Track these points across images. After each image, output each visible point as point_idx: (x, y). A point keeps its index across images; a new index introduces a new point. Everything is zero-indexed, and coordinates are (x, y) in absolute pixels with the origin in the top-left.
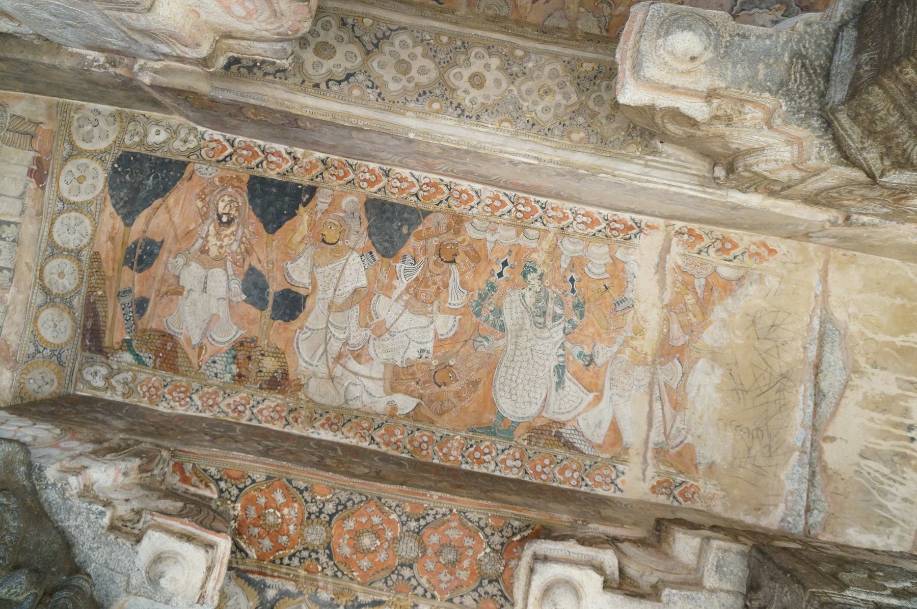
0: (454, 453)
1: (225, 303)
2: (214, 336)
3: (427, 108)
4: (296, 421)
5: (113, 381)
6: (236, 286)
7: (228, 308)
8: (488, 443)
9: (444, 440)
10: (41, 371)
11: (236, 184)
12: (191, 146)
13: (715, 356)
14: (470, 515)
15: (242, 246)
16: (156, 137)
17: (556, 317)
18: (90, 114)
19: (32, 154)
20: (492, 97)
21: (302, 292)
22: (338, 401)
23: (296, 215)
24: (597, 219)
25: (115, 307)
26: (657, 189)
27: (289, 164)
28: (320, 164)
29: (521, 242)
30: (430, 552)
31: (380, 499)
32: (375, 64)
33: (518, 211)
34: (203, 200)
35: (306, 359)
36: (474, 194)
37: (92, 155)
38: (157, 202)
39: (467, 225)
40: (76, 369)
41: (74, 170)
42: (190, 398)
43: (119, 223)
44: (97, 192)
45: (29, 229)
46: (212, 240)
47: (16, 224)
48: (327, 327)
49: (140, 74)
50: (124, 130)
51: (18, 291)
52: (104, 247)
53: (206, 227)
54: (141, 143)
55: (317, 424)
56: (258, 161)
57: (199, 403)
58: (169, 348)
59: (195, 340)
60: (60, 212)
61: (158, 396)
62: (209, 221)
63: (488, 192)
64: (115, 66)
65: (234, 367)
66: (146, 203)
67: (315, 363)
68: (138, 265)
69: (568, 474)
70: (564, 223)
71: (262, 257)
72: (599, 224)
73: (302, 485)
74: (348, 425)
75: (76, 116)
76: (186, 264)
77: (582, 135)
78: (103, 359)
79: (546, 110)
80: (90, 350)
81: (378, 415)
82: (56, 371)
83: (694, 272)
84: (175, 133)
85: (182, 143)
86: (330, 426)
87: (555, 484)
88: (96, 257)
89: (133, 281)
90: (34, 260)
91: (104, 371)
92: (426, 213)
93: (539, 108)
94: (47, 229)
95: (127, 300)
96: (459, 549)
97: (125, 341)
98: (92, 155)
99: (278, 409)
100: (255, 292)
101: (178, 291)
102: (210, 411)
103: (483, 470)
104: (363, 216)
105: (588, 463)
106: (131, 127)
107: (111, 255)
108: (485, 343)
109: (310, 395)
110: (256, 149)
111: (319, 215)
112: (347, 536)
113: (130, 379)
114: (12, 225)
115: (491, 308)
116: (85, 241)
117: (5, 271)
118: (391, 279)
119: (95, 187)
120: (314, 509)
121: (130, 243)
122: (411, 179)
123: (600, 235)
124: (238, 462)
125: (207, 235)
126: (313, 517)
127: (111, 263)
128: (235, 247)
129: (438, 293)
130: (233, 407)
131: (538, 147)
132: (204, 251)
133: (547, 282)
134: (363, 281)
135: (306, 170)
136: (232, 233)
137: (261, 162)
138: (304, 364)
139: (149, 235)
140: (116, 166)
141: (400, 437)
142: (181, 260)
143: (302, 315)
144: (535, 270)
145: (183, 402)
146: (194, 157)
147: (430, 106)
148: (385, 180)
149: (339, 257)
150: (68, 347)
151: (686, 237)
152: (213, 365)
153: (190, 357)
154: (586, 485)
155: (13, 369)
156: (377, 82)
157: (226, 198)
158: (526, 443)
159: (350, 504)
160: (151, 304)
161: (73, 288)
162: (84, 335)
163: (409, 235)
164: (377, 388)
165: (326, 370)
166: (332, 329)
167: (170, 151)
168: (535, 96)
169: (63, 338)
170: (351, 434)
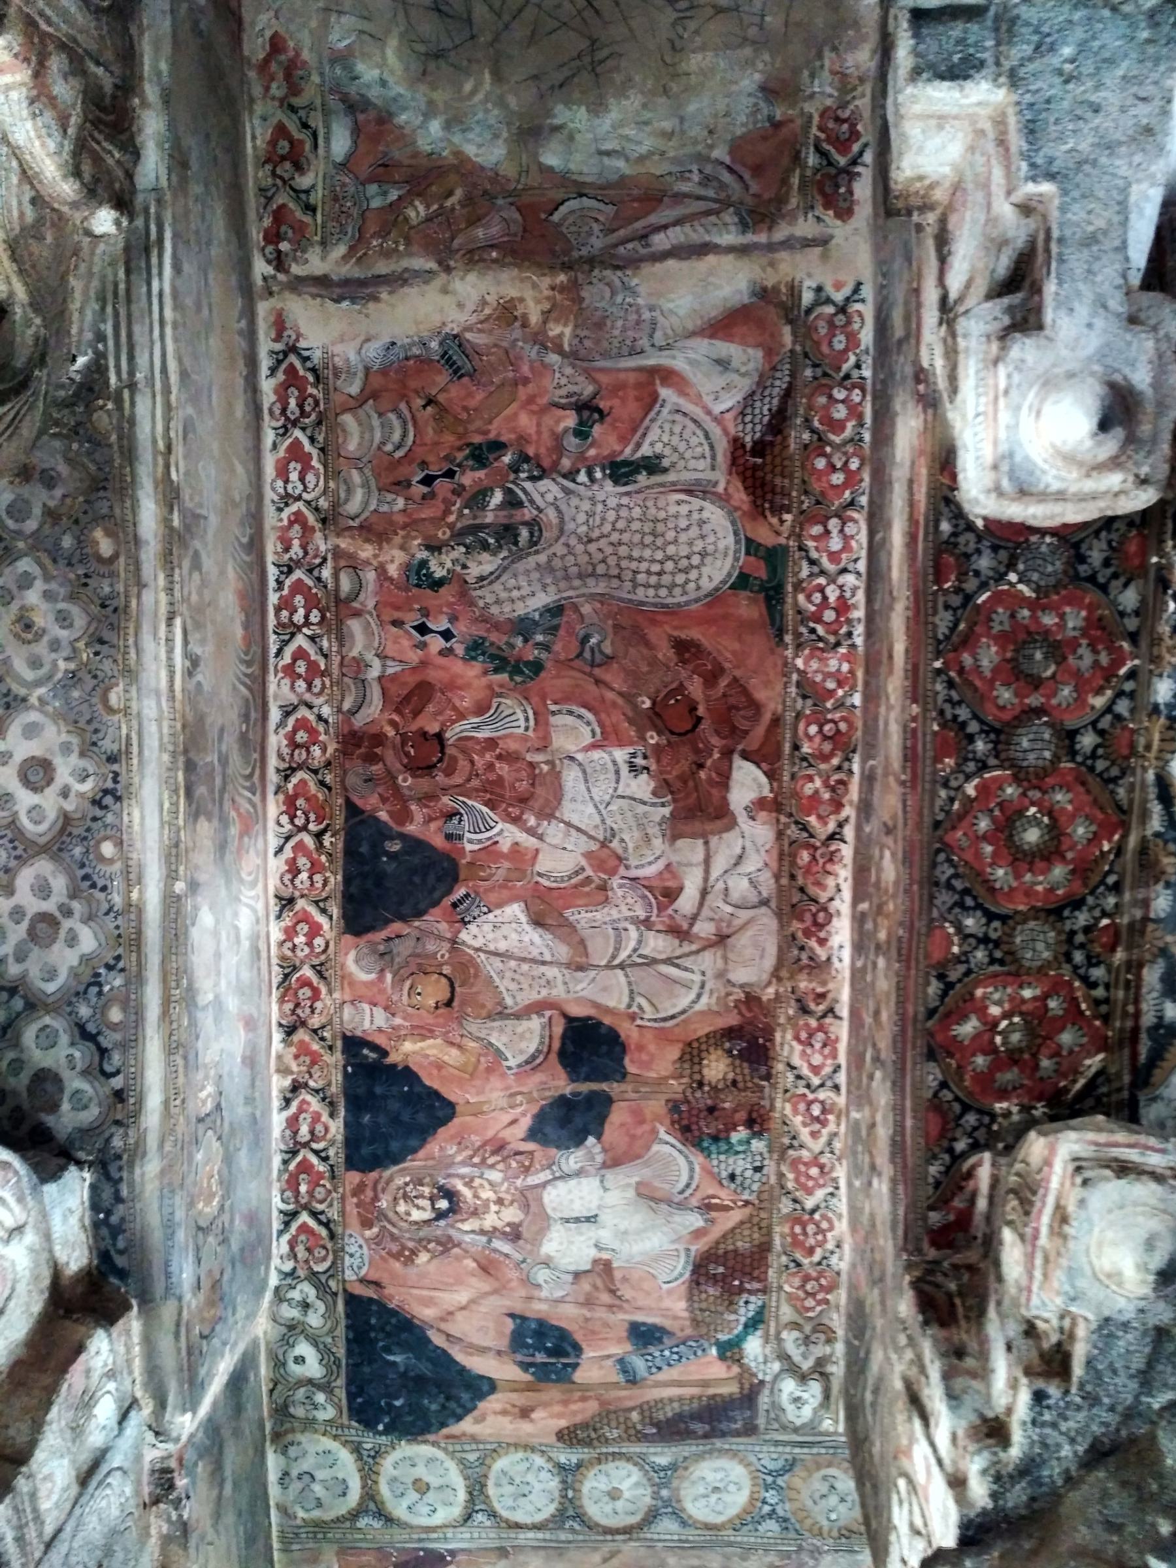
0: (833, 665)
2: (681, 1186)
3: (118, 866)
4: (822, 996)
6: (573, 1159)
7: (618, 1170)
8: (801, 598)
9: (808, 690)
10: (809, 1503)
11: (369, 1193)
13: (530, 132)
14: (942, 630)
15: (490, 1161)
17: (512, 502)
20: (64, 737)
21: (559, 1029)
22: (767, 921)
24: (289, 449)
25: (658, 1385)
26: (177, 351)
27: (309, 1098)
28: (296, 1038)
29: (371, 604)
30: (1034, 700)
31: (937, 825)
32: (51, 988)
33: (307, 623)
34: (414, 1253)
35: (692, 996)
36: (291, 721)
37: (369, 1473)
38: (438, 1340)
39: (359, 721)
41: (405, 1503)
42: (813, 1211)
43: (492, 1403)
44: (440, 1454)
46: (490, 1221)
48: (621, 966)
50: (309, 1424)
52: (547, 1421)
53: (467, 1238)
55: (822, 953)
56: (314, 1160)
57: (820, 1194)
58: (721, 1270)
59: (696, 1221)
60: (493, 1514)
63: (279, 690)
65: (735, 1137)
66: (443, 1359)
67: (697, 978)
68: (567, 1355)
69: (840, 412)
70: (311, 519)
71: (506, 1118)
72: (297, 443)
73: (934, 988)
74: (812, 890)
75: (301, 1514)
76: (547, 1263)
77: (98, 534)
78: (766, 1392)
79: (63, 619)
81: (780, 835)
82: (803, 1474)
83: (355, 212)
85: (310, 1312)
86: (821, 926)
87: (867, 436)
88: (567, 1436)
90: (596, 1549)
92: (352, 809)
93: (63, 634)
94: (531, 1535)
96: (1020, 639)
97: (722, 1357)
98: (369, 1473)
99: (804, 1035)
100: (578, 1121)
101: (603, 1268)
102: (832, 1169)
103: (860, 597)
104: (383, 934)
105: (808, 373)
106: (299, 1412)
107: (557, 1408)
108: (593, 641)
109: (765, 977)
110: (292, 1167)
111: (398, 1021)
112: (1028, 877)
113: (796, 1334)
115: (519, 642)
116: (539, 1461)
118: (501, 855)
119: (431, 1460)
120: (980, 955)
121: (528, 1377)
122: (288, 852)
123: (321, 438)
124: (909, 1123)
125: (482, 1232)
126: (998, 954)
127: (574, 1407)
128: (495, 1176)
129: (509, 757)
130: (817, 1126)
131: (146, 627)
132: (514, 1234)
133: (443, 534)
134: (515, 910)
135: (314, 1063)
136: (469, 1184)
137: (316, 1153)
138: (704, 1000)
139: (504, 1343)
140: (381, 1427)
141: (818, 783)
142: (542, 1275)
143: (607, 1021)
144: (424, 564)
145: (824, 1225)
146: (332, 1284)
147: (111, 861)
148: (301, 904)
149: (477, 967)
150: (753, 1459)
151: (284, 246)
152: (739, 1180)
153: (730, 1224)
154: (858, 366)
156: (87, 978)
157: (402, 1207)
158: (788, 517)
159: (958, 884)
160: (640, 1318)
161: (635, 1469)
162: (723, 1434)
163: (403, 837)
164: (726, 847)
165: (708, 956)
166: (623, 955)
167: (331, 1331)
168: (41, 648)
169: (737, 1471)
170: (830, 882)
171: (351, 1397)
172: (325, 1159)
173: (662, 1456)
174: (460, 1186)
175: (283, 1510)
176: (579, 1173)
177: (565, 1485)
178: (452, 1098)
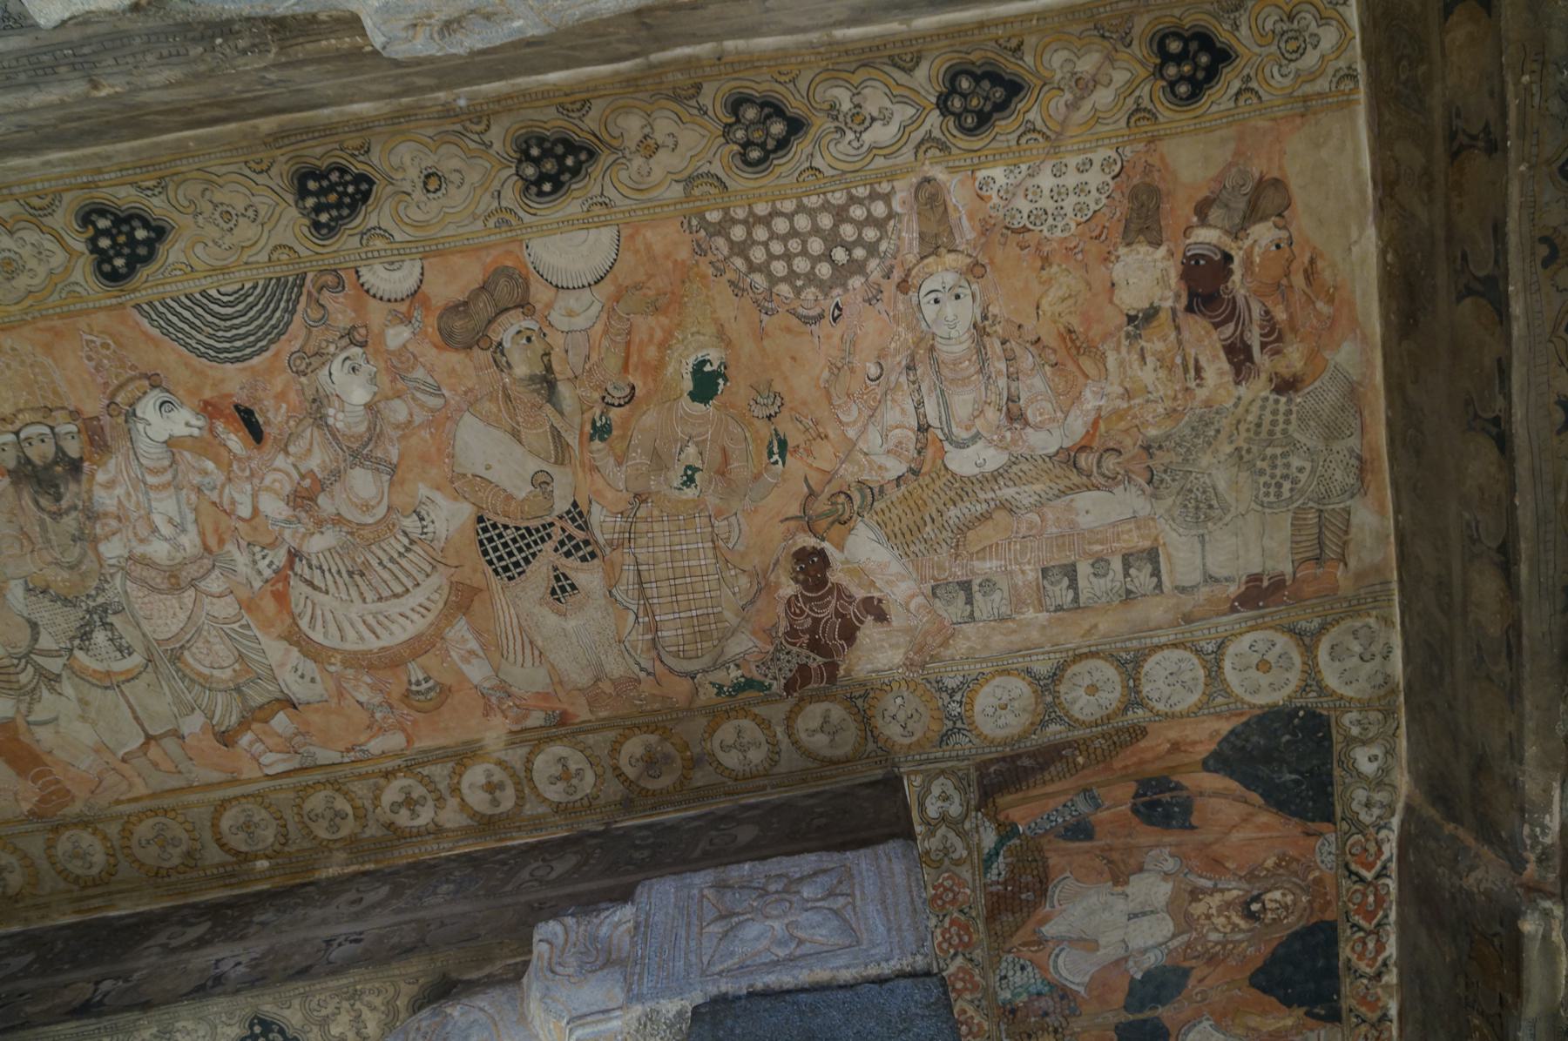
1: (1121, 953)
2: (1063, 954)
5: (943, 830)
6: (1152, 960)
10: (921, 709)
11: (1316, 905)
12: (1365, 817)
15: (1218, 948)
16: (1365, 761)
18: (1382, 641)
19: (1288, 568)
23: (1289, 1006)
25: (1065, 792)
27: (1368, 970)
28: (1379, 1013)
34: (1278, 865)
37: (1311, 671)
38: (1256, 798)
40: (942, 765)
41: (1277, 650)
42: (956, 954)
43: (1203, 751)
44: (1248, 698)
45: (1156, 611)
46: (1216, 900)
47: (1159, 585)
49: (1536, 915)
50: (1365, 706)
51: (1044, 627)
53: (1234, 884)
54: (1350, 741)
56: (1362, 923)
58: (1023, 896)
59: (1048, 930)
60: (1199, 652)
61: (943, 907)
62: (1246, 886)
64: (1539, 861)
65: (1024, 997)
68: (1144, 804)
71: (1208, 982)
75: (1372, 621)
76: (1167, 876)
80: (981, 776)
84: (1378, 784)
85: (1364, 800)
88: (1138, 732)
89: (1115, 806)
90: (1104, 636)
91: (955, 809)
94: (1164, 640)
95: (1083, 807)
97: (1014, 826)
98: (1311, 671)
101: (1119, 878)
106: (1374, 716)
107: (1149, 755)
113: (956, 856)
114: (1155, 580)
116: (1160, 707)
117: (1071, 594)
119: (1255, 692)
121: (1175, 778)
125: (1222, 891)
127: (1135, 759)
128: (1214, 936)
132: (1195, 894)
135: (1364, 997)
136: (1235, 926)
137: (1361, 929)
139: (1198, 802)
140: (1301, 713)
142: (1171, 865)
145: (945, 946)
146: (1345, 826)
153: (1020, 933)
155: (909, 664)
160: (1086, 845)
161: (1077, 715)
162: (1004, 759)
169: (988, 727)
171: (1328, 737)
172: (1353, 925)
173: (1055, 731)
174: (1243, 924)
175: (1387, 621)
176: (1145, 951)
177: (1136, 690)
178: (1253, 990)
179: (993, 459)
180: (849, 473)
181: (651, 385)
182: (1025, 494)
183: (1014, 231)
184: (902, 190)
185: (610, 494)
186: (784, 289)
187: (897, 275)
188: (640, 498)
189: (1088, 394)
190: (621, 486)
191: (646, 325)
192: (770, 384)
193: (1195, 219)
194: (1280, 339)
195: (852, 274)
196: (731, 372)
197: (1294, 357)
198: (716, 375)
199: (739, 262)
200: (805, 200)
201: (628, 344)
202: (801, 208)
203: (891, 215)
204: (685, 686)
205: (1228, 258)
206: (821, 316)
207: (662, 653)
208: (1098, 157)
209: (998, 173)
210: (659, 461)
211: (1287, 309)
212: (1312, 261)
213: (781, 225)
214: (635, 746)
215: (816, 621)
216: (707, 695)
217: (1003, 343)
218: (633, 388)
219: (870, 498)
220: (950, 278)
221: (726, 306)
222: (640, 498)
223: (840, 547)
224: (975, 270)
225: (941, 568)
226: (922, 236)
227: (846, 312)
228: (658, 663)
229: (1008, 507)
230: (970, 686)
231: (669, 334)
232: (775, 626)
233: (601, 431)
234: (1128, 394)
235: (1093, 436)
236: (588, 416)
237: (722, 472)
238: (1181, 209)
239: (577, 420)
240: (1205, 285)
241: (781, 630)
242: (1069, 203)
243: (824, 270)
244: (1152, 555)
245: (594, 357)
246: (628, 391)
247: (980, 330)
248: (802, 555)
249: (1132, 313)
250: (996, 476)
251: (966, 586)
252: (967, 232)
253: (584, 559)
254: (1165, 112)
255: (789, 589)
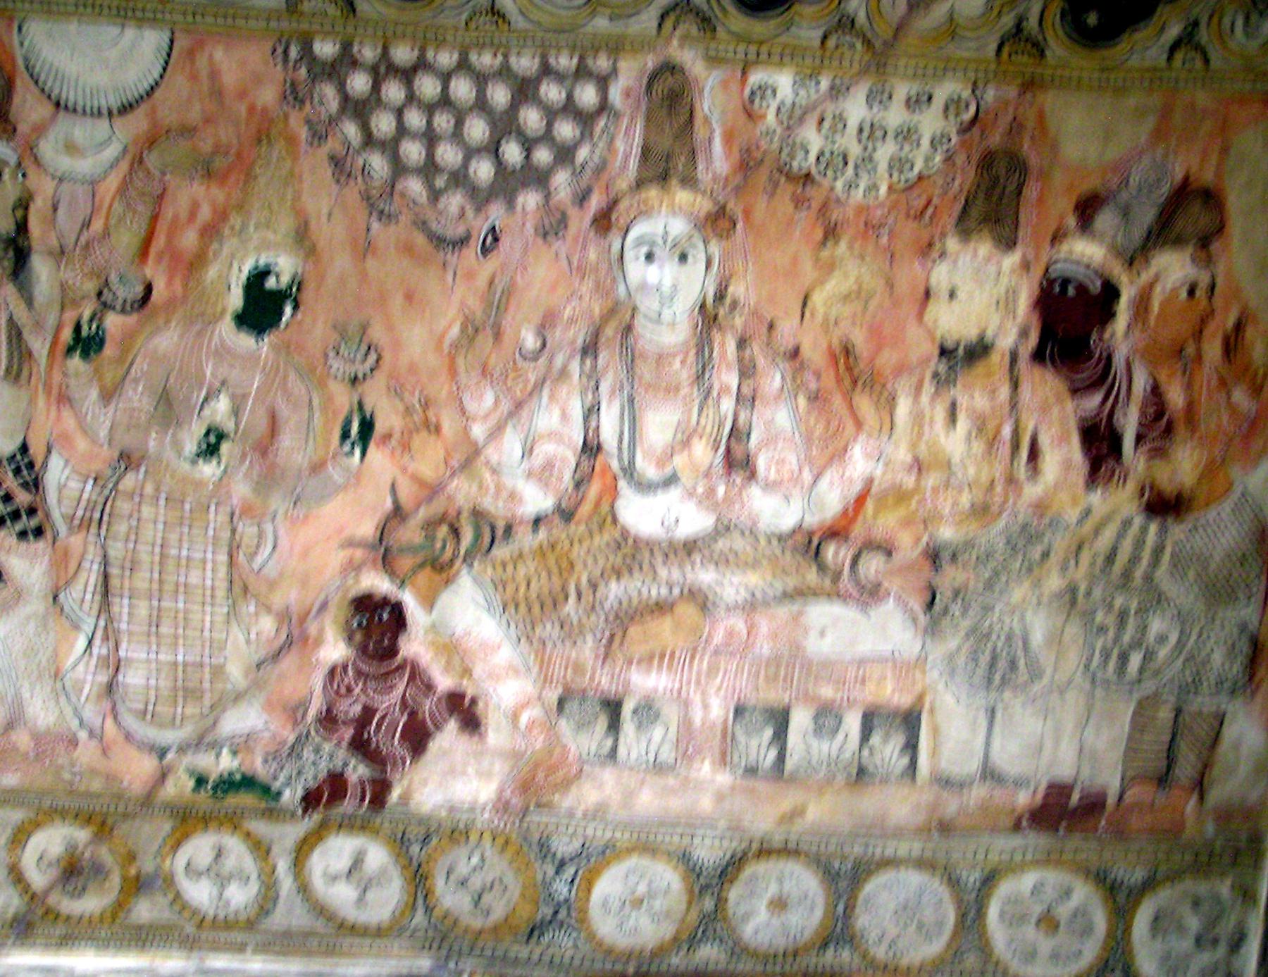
19: (1113, 784)
45: (900, 806)
60: (953, 882)
116: (880, 953)
117: (773, 754)
155: (502, 806)
169: (606, 927)
179: (693, 520)
180: (462, 492)
181: (179, 291)
182: (731, 586)
183: (790, 177)
184: (629, 75)
185: (82, 444)
186: (415, 186)
187: (596, 202)
188: (127, 460)
189: (857, 452)
190: (103, 434)
191: (191, 196)
192: (364, 329)
193: (1071, 221)
194: (1169, 430)
195: (524, 185)
196: (307, 296)
197: (1183, 466)
198: (279, 297)
199: (351, 130)
200: (473, 57)
201: (155, 218)
202: (463, 65)
203: (604, 106)
204: (146, 766)
205: (1111, 292)
206: (463, 241)
207: (120, 707)
208: (945, 90)
209: (784, 82)
210: (168, 408)
211: (1189, 386)
212: (1239, 327)
213: (428, 87)
214: (51, 841)
215: (368, 712)
216: (179, 786)
217: (742, 343)
218: (149, 289)
219: (487, 540)
220: (678, 227)
221: (321, 197)
222: (127, 460)
223: (429, 602)
224: (717, 222)
225: (578, 669)
226: (646, 152)
227: (505, 242)
228: (109, 722)
229: (701, 600)
230: (592, 860)
231: (221, 216)
232: (304, 705)
233: (87, 343)
234: (919, 466)
235: (853, 520)
236: (70, 317)
237: (265, 446)
238: (1049, 201)
239: (51, 320)
240: (1069, 326)
241: (312, 713)
242: (885, 152)
243: (483, 170)
244: (910, 721)
245: (97, 225)
246: (139, 289)
247: (708, 318)
248: (366, 605)
249: (950, 344)
250: (689, 547)
251: (613, 708)
252: (717, 161)
253: (23, 535)
254: (1058, 48)
255: (335, 650)
